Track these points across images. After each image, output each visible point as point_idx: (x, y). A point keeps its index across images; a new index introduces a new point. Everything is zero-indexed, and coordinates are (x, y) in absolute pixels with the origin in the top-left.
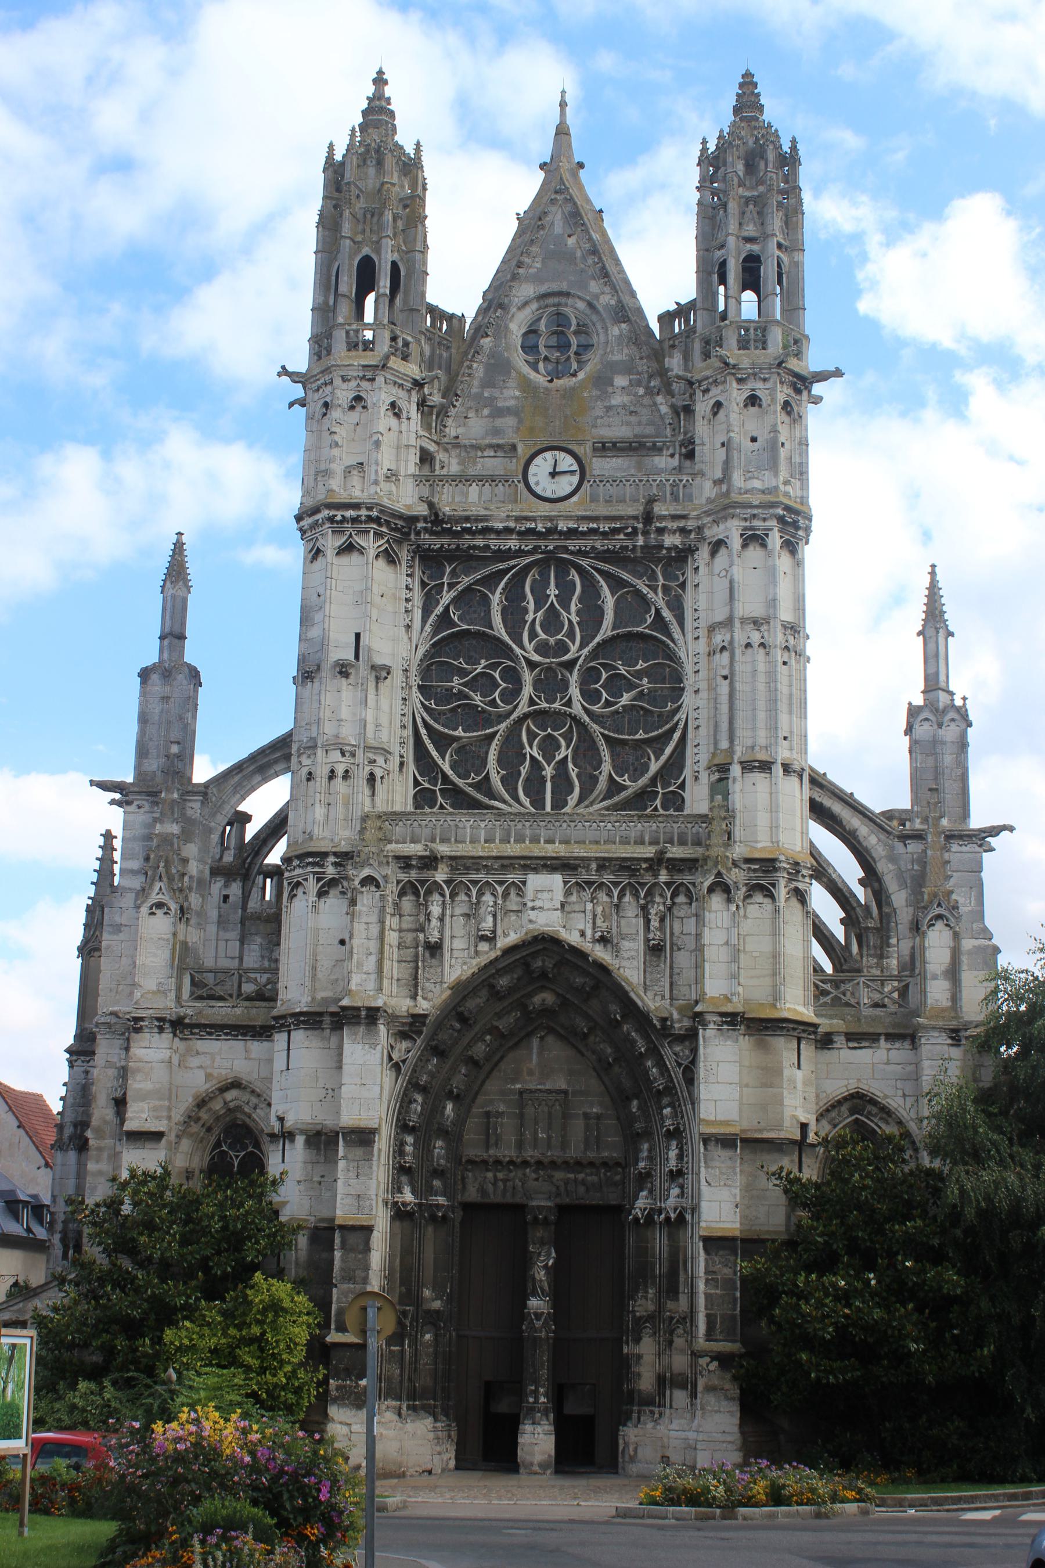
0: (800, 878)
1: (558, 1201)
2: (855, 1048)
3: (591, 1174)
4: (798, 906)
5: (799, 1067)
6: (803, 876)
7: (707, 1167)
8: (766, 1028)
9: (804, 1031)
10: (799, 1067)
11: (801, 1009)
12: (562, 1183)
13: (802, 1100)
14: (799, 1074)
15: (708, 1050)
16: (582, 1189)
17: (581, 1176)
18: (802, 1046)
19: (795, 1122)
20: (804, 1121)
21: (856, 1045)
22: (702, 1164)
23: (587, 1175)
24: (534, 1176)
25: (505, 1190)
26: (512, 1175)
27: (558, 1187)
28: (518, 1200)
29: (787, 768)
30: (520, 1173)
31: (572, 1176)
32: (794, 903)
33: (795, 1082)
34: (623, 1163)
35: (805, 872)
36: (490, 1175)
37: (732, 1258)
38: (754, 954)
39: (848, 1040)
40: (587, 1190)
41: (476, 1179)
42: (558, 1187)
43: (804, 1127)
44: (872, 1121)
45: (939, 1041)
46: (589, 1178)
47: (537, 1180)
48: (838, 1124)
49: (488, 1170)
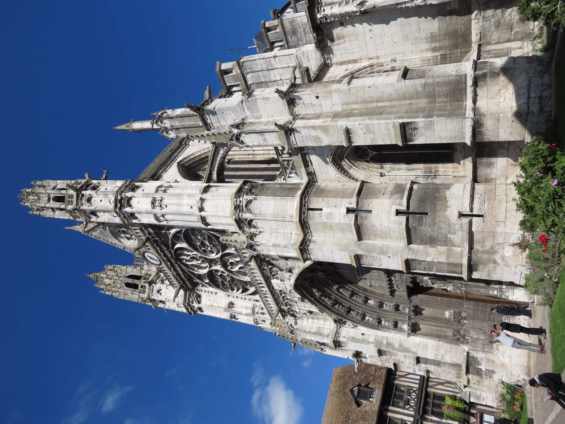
0: (241, 204)
2: (311, 163)
4: (253, 202)
5: (321, 209)
6: (240, 201)
7: (373, 265)
8: (306, 227)
9: (305, 206)
10: (321, 209)
11: (295, 207)
13: (336, 209)
14: (325, 210)
15: (320, 258)
18: (311, 207)
19: (346, 217)
20: (345, 211)
21: (310, 163)
22: (372, 267)
29: (201, 209)
32: (252, 206)
33: (328, 213)
35: (238, 203)
37: (417, 261)
38: (277, 226)
39: (309, 166)
43: (349, 211)
44: (345, 151)
45: (294, 139)
48: (350, 166)
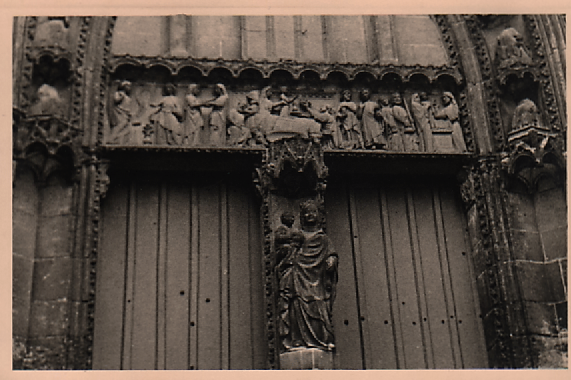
1: (328, 148)
3: (393, 104)
12: (332, 118)
16: (375, 130)
17: (370, 105)
23: (380, 101)
24: (270, 103)
25: (208, 124)
26: (221, 100)
27: (324, 124)
28: (239, 140)
30: (240, 99)
31: (353, 105)
34: (459, 78)
36: (171, 100)
40: (387, 132)
41: (142, 108)
42: (324, 124)
46: (386, 110)
47: (274, 111)
49: (166, 93)
